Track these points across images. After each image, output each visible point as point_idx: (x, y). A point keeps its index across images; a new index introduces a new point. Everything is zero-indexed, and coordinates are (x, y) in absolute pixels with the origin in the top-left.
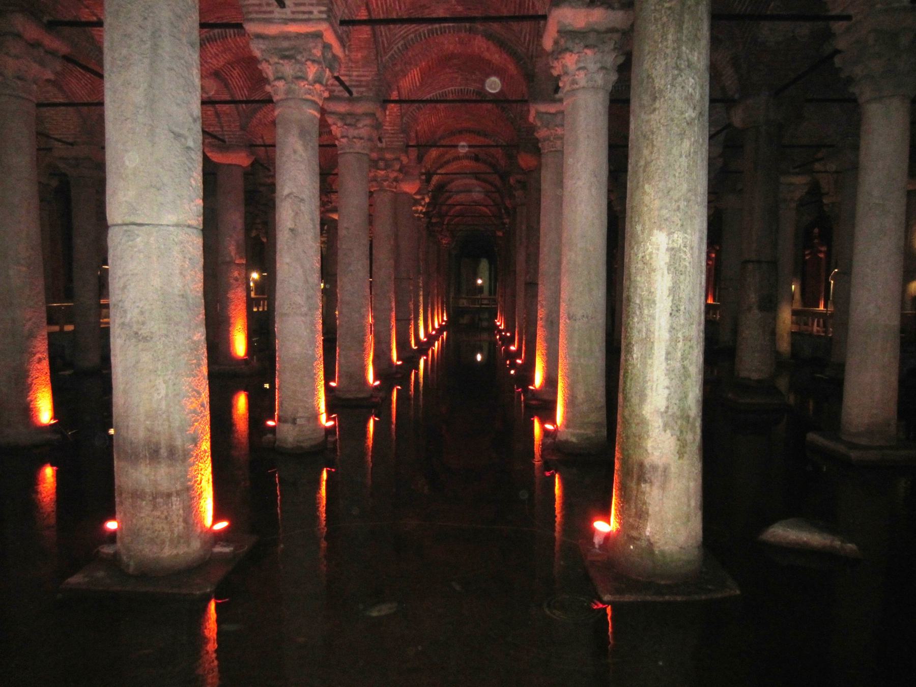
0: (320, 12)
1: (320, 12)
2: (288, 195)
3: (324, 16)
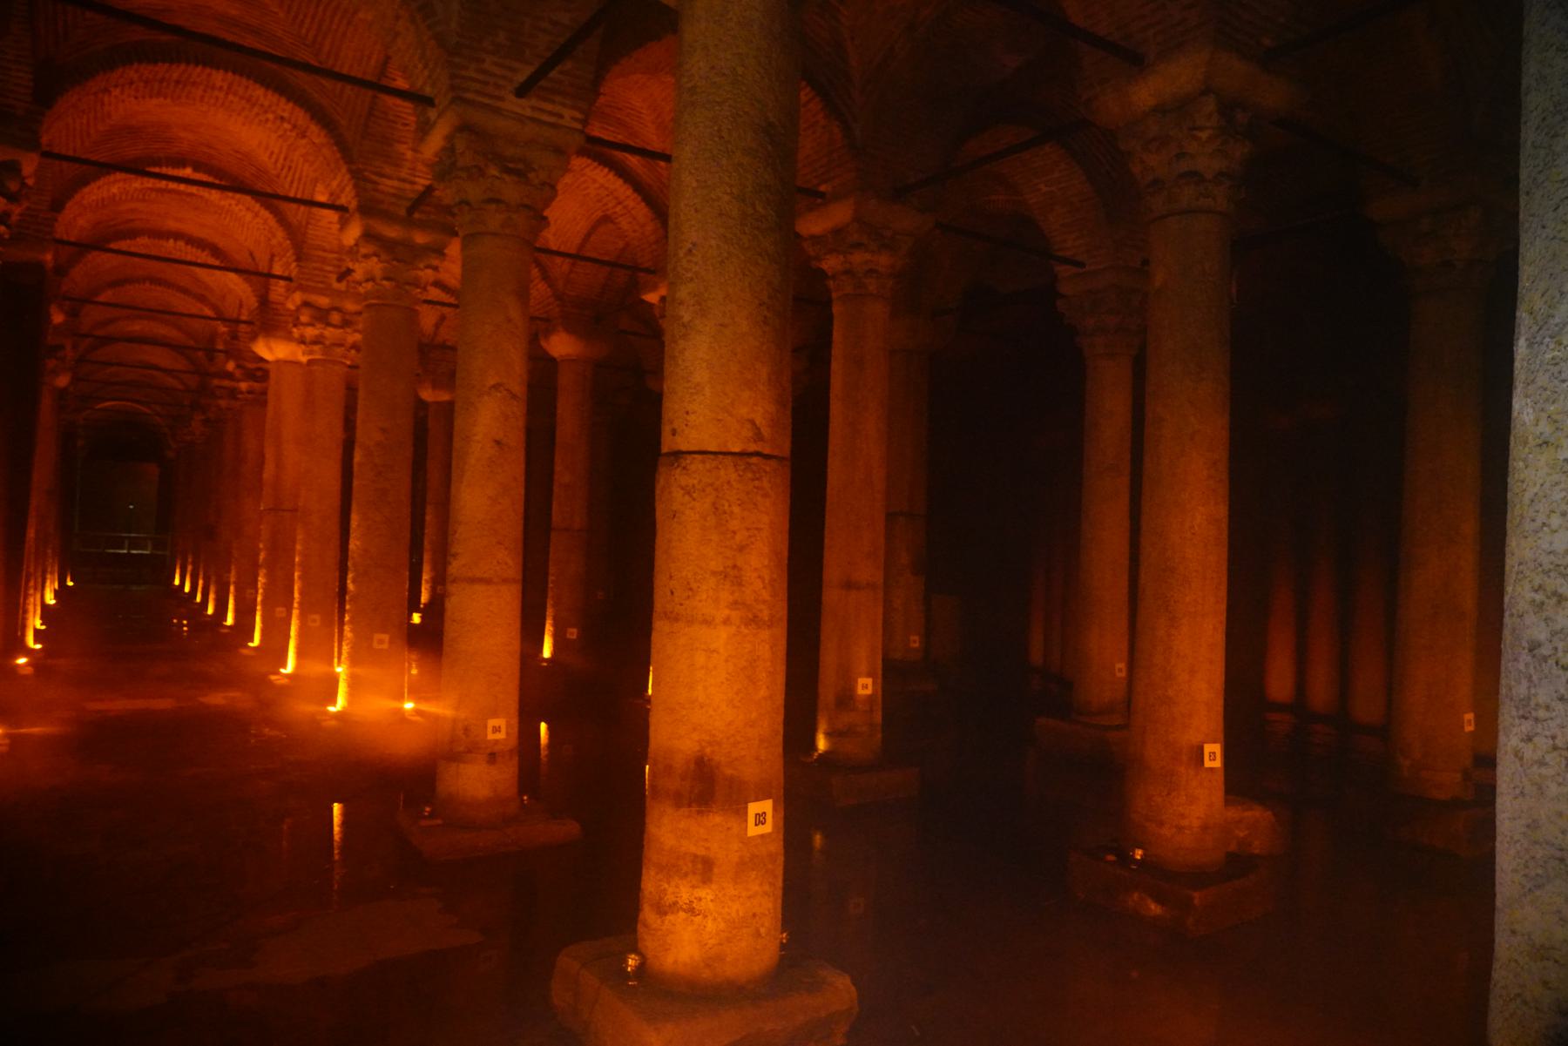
0: (576, 120)
1: (576, 120)
2: (496, 387)
3: (579, 126)
